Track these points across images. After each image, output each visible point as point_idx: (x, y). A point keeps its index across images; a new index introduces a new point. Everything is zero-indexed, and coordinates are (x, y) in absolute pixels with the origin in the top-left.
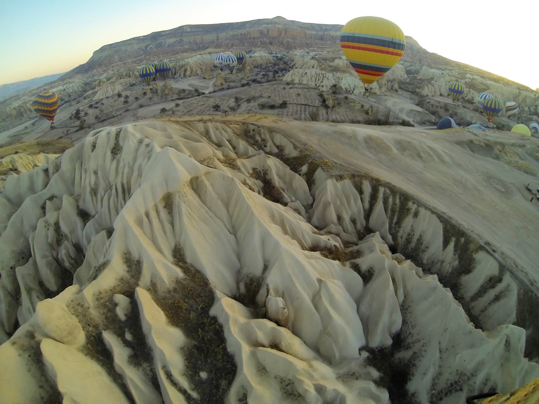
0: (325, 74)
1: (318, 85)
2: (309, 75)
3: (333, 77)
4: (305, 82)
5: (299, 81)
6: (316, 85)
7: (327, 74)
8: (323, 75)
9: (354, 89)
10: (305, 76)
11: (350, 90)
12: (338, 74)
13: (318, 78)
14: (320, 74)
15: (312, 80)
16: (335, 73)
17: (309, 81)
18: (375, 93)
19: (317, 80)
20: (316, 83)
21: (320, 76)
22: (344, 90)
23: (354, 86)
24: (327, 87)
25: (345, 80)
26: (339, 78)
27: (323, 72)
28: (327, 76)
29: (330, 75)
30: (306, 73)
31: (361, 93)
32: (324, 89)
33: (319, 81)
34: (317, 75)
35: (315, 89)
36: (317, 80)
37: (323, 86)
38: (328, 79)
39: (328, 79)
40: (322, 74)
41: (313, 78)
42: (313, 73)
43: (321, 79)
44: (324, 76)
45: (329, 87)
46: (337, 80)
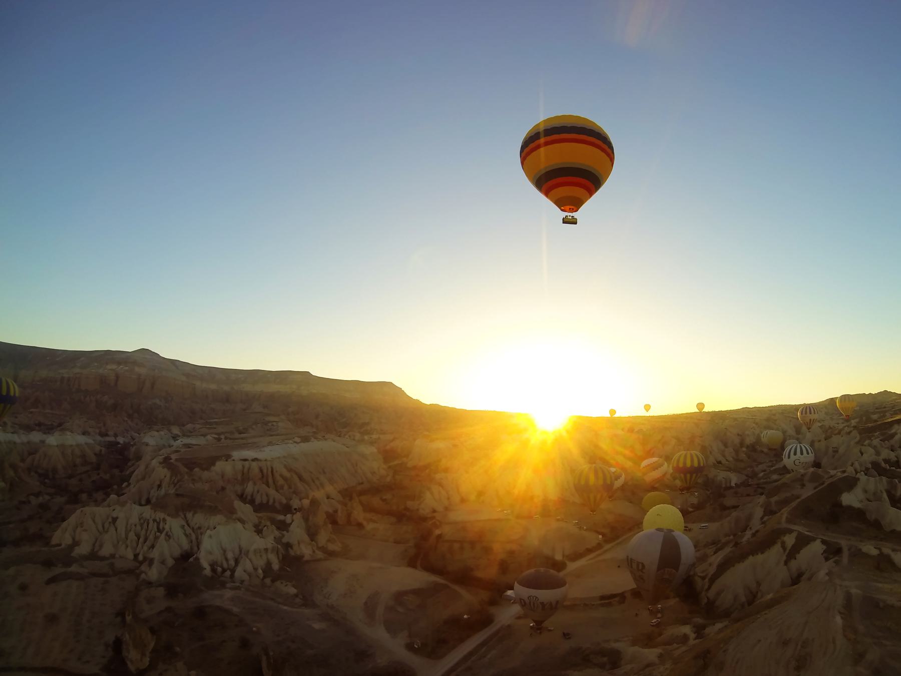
0: (164, 520)
1: (141, 558)
2: (121, 524)
3: (183, 527)
4: (106, 551)
5: (94, 545)
6: (136, 556)
7: (168, 519)
8: (158, 524)
9: (237, 562)
10: (112, 529)
11: (225, 566)
12: (198, 519)
13: (143, 532)
14: (151, 522)
15: (128, 542)
16: (189, 515)
17: (120, 543)
18: (299, 559)
19: (141, 540)
20: (138, 551)
21: (150, 525)
22: (208, 571)
23: (237, 551)
24: (163, 562)
25: (210, 537)
26: (199, 528)
27: (160, 515)
28: (167, 527)
29: (174, 525)
30: (115, 520)
31: (256, 569)
32: (154, 573)
33: (145, 542)
34: (142, 525)
35: (130, 572)
36: (141, 540)
37: (151, 562)
38: (168, 536)
39: (168, 536)
40: (154, 520)
41: (132, 535)
42: (134, 519)
43: (151, 537)
44: (161, 527)
45: (170, 562)
46: (194, 537)
